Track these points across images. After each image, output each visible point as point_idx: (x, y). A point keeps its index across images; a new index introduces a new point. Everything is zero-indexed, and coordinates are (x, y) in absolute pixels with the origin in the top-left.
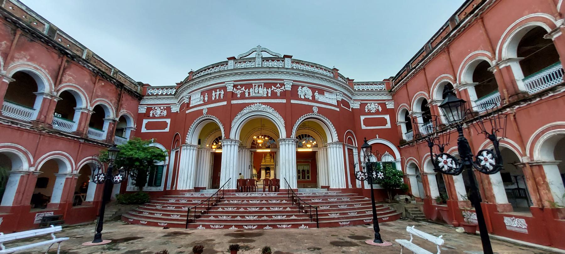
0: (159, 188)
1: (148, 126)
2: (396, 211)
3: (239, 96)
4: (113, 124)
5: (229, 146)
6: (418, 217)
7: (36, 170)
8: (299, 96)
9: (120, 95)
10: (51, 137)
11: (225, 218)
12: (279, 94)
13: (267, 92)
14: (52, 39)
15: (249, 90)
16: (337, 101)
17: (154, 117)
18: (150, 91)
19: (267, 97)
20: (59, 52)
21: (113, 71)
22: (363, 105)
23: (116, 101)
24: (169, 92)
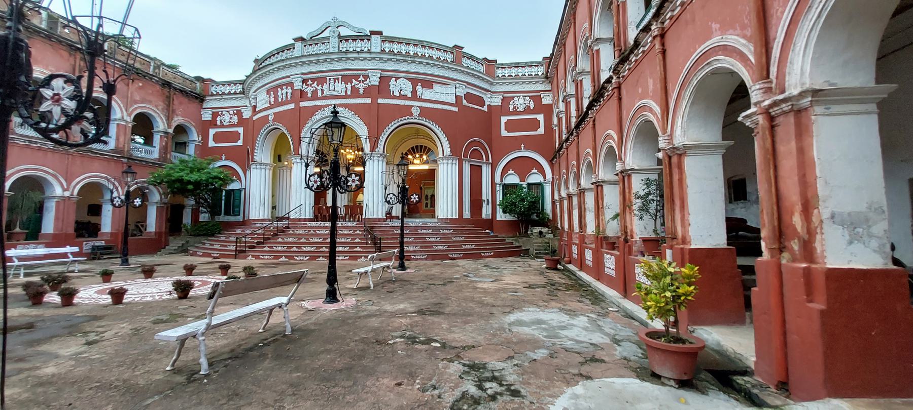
0: (238, 217)
1: (217, 138)
2: (521, 246)
3: (309, 95)
4: (165, 137)
6: (540, 253)
7: (72, 194)
9: (169, 97)
10: (82, 156)
11: (280, 249)
12: (361, 92)
13: (346, 88)
14: (54, 33)
15: (322, 87)
16: (456, 97)
17: (222, 126)
18: (213, 90)
19: (346, 97)
20: (68, 48)
21: (152, 64)
23: (165, 106)
24: (233, 89)
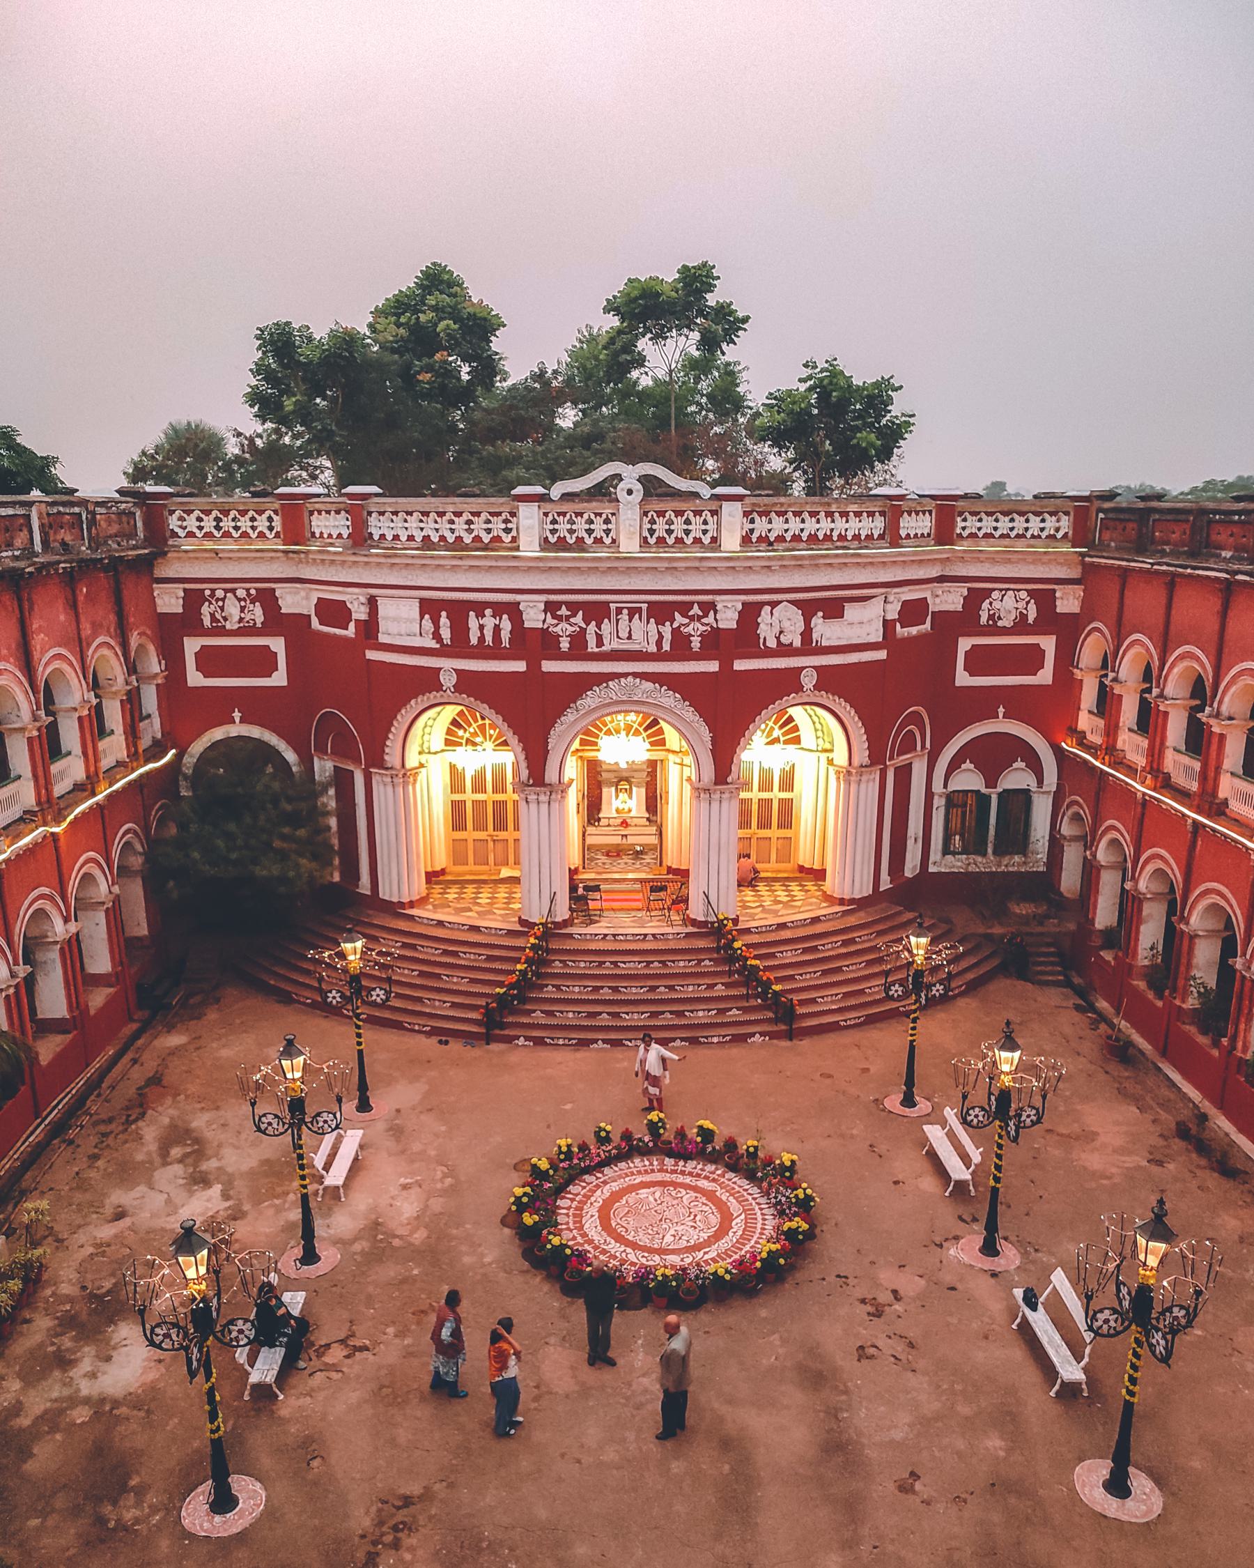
3: (565, 645)
5: (544, 807)
8: (761, 641)
12: (696, 643)
13: (659, 633)
17: (221, 631)
19: (659, 656)
22: (975, 598)
